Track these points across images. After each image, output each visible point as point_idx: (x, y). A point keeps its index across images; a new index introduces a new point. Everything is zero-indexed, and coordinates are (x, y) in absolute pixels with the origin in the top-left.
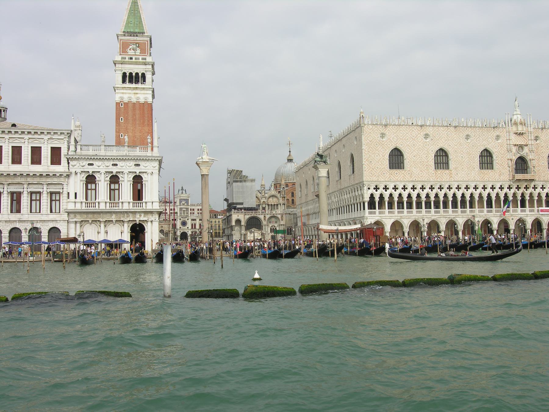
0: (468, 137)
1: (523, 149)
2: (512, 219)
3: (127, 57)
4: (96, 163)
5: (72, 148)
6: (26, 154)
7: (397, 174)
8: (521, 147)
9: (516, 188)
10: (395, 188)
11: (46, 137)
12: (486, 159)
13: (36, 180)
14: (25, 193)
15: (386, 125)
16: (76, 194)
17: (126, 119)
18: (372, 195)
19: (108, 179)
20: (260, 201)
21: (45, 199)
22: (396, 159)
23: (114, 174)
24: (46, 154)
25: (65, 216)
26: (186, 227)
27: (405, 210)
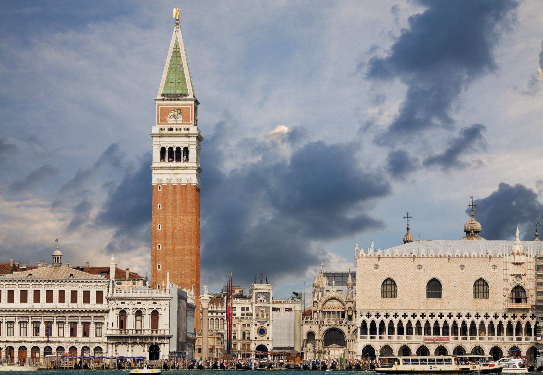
0: (462, 267)
1: (521, 277)
2: (505, 347)
3: (167, 127)
5: (111, 291)
6: (80, 296)
7: (388, 302)
8: (519, 276)
9: (512, 317)
10: (387, 316)
11: (93, 284)
12: (481, 287)
13: (86, 314)
14: (80, 323)
16: (113, 323)
17: (165, 206)
18: (364, 321)
19: (135, 313)
20: (345, 307)
22: (389, 287)
24: (93, 296)
25: (106, 340)
26: (265, 338)
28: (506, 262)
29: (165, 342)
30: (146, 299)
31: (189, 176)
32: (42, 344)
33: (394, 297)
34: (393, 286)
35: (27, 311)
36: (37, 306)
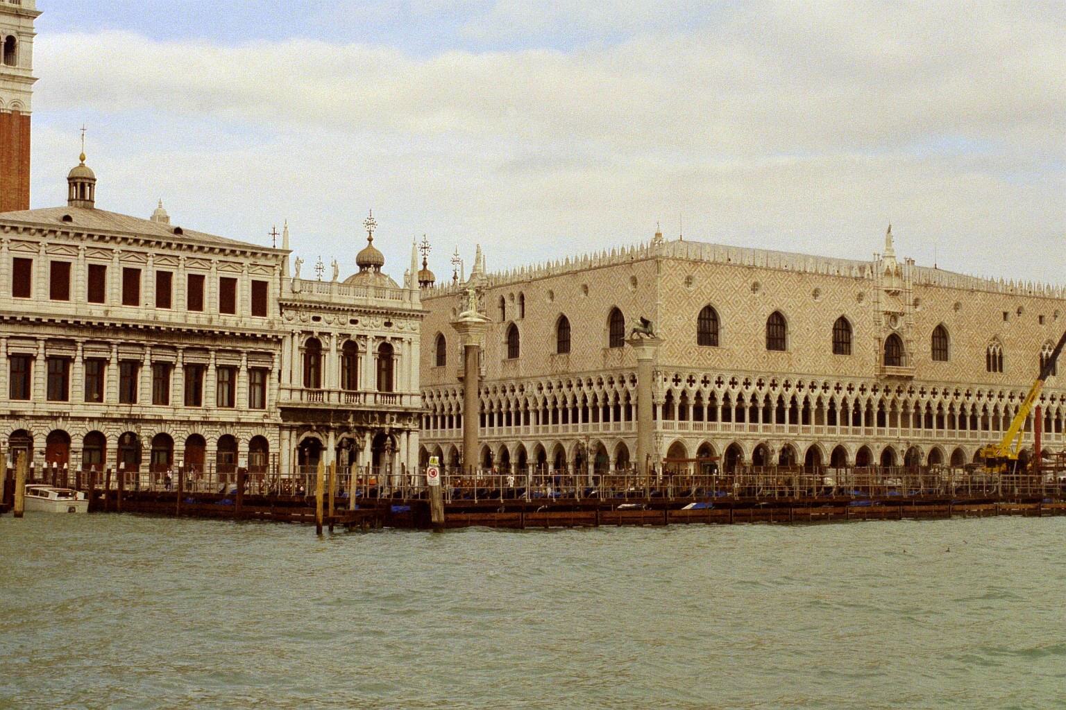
0: (816, 293)
1: (896, 320)
2: (878, 447)
4: (325, 317)
7: (709, 354)
8: (894, 316)
11: (246, 262)
13: (228, 346)
14: (212, 370)
15: (695, 262)
19: (341, 347)
21: (242, 383)
22: (709, 328)
23: (352, 339)
24: (243, 294)
25: (277, 417)
27: (719, 422)
28: (877, 288)
29: (411, 426)
30: (368, 312)
31: (17, 96)
32: (113, 425)
33: (714, 345)
34: (711, 322)
35: (77, 326)
36: (96, 311)
